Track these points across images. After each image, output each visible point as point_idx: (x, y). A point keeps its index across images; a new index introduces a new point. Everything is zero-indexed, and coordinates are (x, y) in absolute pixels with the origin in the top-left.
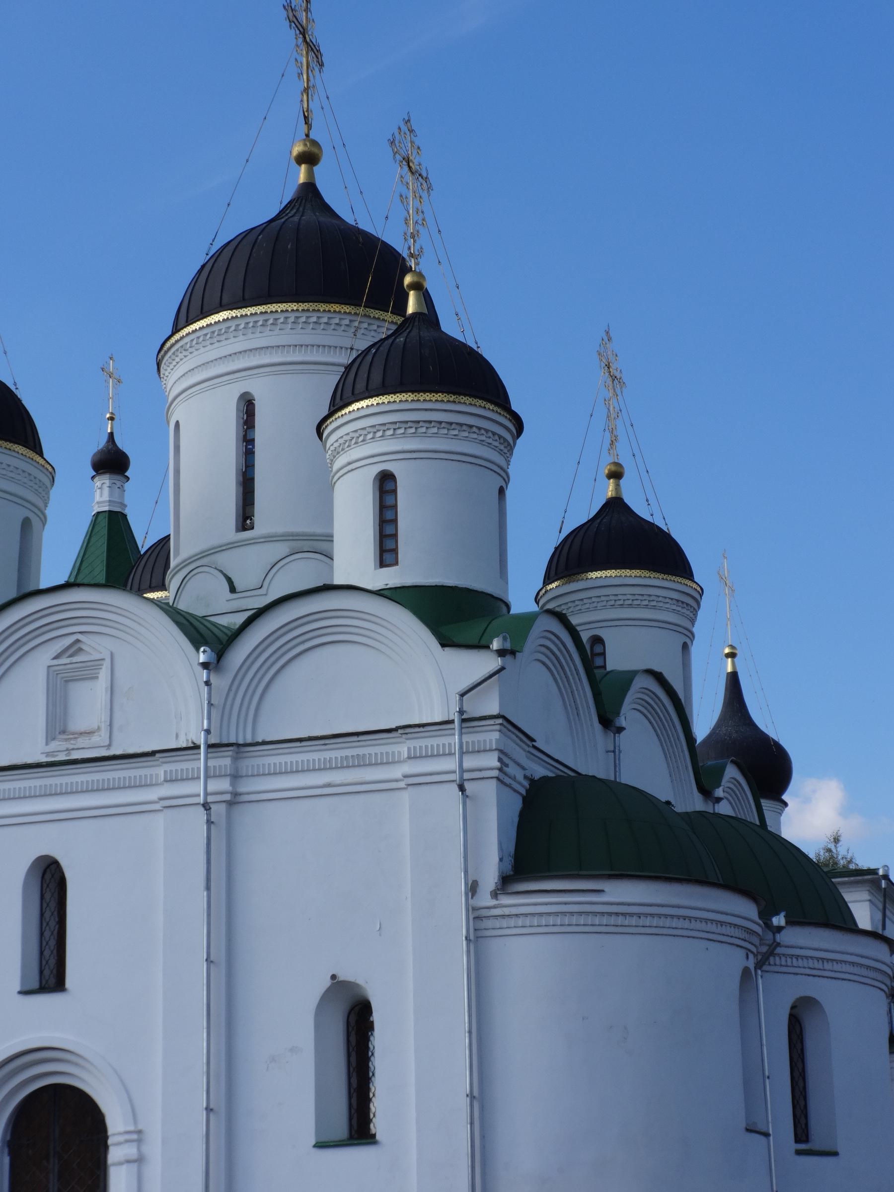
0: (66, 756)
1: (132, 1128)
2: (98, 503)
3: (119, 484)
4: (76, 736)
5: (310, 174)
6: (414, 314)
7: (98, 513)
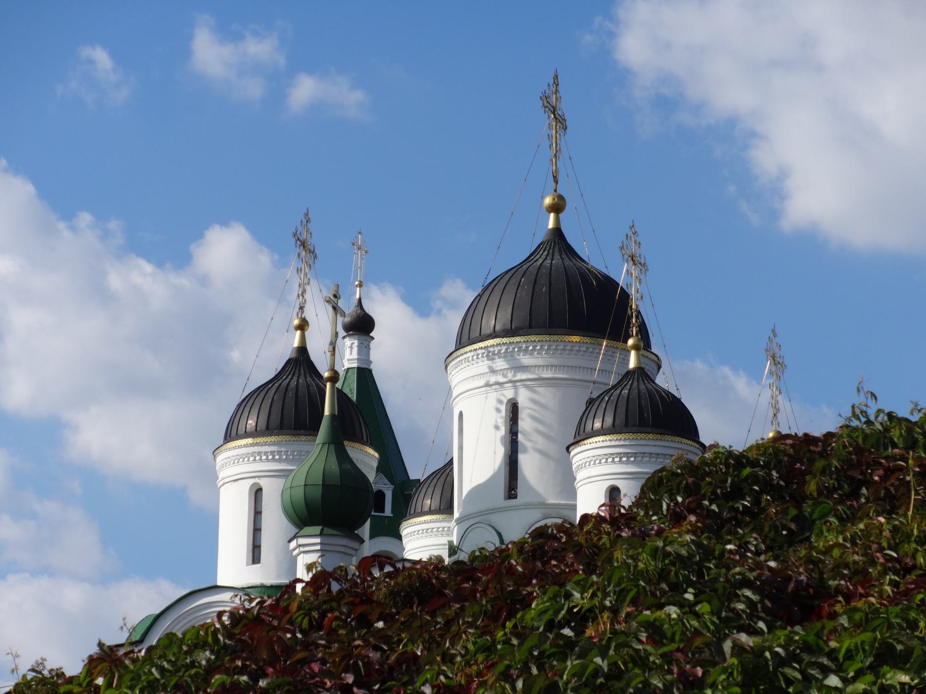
2: (348, 360)
3: (366, 343)
5: (557, 220)
7: (348, 369)
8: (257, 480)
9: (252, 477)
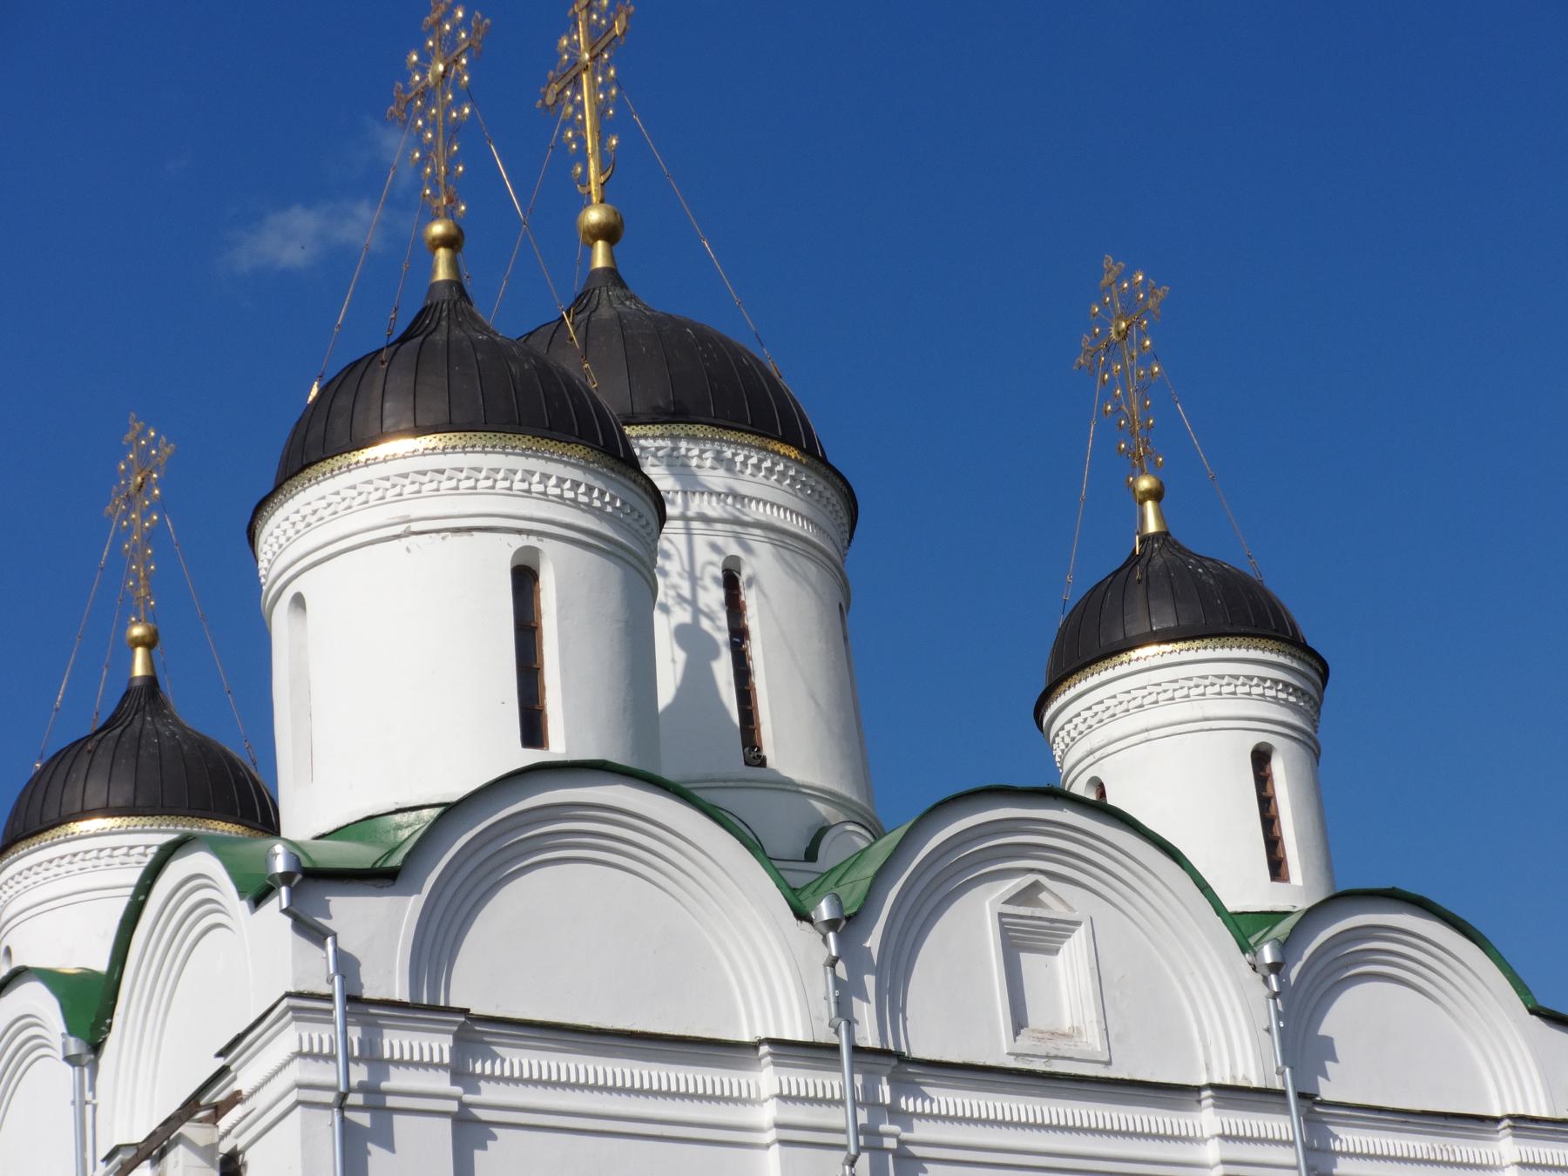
0: (1046, 1066)
4: (1047, 1036)
8: (532, 541)
9: (519, 532)
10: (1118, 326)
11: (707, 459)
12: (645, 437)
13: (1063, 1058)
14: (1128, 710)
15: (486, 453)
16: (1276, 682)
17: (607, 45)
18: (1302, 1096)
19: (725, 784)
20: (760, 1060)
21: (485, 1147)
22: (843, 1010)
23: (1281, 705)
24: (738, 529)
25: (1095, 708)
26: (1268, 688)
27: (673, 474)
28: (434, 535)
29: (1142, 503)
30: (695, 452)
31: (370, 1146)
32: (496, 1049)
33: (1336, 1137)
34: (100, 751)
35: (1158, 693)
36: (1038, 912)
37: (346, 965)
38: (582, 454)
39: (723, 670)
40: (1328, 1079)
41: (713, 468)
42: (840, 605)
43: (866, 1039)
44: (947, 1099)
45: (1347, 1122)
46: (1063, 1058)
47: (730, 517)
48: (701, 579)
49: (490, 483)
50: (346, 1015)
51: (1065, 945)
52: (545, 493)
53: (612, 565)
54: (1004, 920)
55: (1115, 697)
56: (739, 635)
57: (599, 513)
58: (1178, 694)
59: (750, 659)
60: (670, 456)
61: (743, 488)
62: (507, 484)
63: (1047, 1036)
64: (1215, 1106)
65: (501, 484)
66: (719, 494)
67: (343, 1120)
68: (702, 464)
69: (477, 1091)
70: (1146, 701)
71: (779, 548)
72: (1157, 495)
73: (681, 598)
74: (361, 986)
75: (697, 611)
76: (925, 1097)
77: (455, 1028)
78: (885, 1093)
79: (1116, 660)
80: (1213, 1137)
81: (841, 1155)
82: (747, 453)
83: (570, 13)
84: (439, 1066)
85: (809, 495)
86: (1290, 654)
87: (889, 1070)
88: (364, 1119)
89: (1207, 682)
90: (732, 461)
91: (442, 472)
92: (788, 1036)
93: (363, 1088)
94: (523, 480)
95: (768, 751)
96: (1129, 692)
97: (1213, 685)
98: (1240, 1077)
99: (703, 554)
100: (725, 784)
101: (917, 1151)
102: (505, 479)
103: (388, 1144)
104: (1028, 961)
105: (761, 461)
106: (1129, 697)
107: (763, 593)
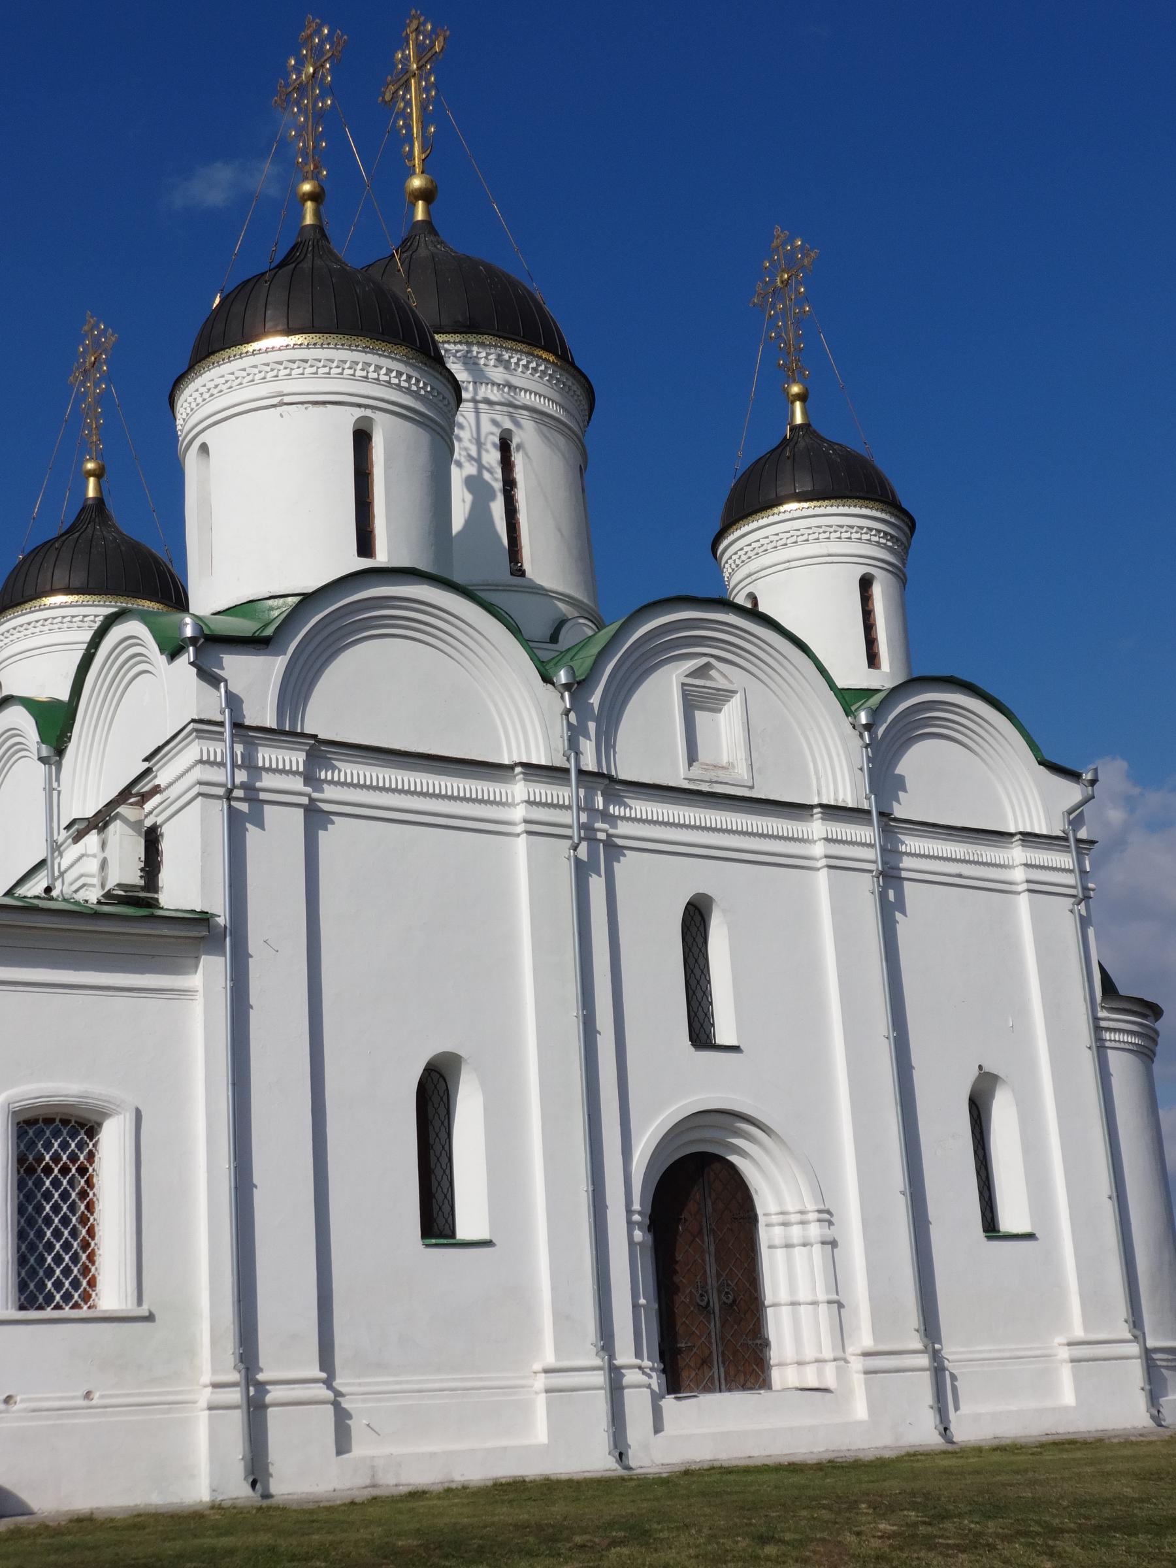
1: (822, 1207)
4: (711, 768)
6: (800, 425)
8: (368, 413)
9: (359, 406)
10: (782, 277)
11: (491, 360)
12: (448, 342)
13: (721, 783)
14: (776, 547)
15: (338, 349)
16: (879, 531)
17: (430, 59)
18: (881, 814)
19: (497, 588)
20: (515, 776)
21: (326, 829)
22: (573, 745)
23: (882, 547)
24: (511, 410)
25: (754, 545)
26: (874, 535)
27: (467, 369)
28: (299, 406)
29: (793, 402)
30: (483, 354)
31: (248, 825)
32: (335, 763)
33: (903, 843)
34: (64, 548)
35: (798, 536)
36: (708, 683)
37: (233, 702)
38: (404, 352)
39: (498, 508)
40: (900, 804)
41: (495, 366)
42: (580, 466)
43: (588, 765)
44: (641, 807)
45: (911, 833)
46: (721, 783)
47: (507, 402)
48: (484, 444)
49: (339, 370)
50: (232, 736)
51: (726, 707)
52: (378, 379)
53: (423, 432)
54: (686, 688)
55: (767, 537)
56: (509, 484)
57: (415, 395)
58: (811, 537)
59: (517, 501)
60: (465, 356)
61: (515, 381)
62: (351, 372)
63: (711, 768)
64: (822, 819)
65: (347, 372)
66: (499, 385)
67: (230, 807)
68: (487, 363)
69: (322, 791)
70: (789, 541)
71: (540, 425)
72: (803, 397)
73: (470, 457)
74: (244, 717)
75: (481, 467)
76: (626, 805)
77: (308, 748)
78: (599, 802)
79: (770, 512)
80: (820, 840)
81: (569, 843)
82: (519, 356)
83: (404, 34)
84: (297, 773)
85: (562, 388)
86: (890, 512)
87: (602, 786)
88: (244, 807)
89: (832, 530)
90: (508, 362)
91: (306, 361)
92: (534, 761)
93: (243, 786)
94: (363, 370)
95: (527, 566)
96: (777, 534)
97: (835, 532)
98: (840, 800)
99: (486, 427)
100: (497, 587)
101: (620, 842)
102: (350, 368)
103: (260, 825)
104: (700, 716)
105: (528, 363)
106: (777, 538)
107: (529, 457)
